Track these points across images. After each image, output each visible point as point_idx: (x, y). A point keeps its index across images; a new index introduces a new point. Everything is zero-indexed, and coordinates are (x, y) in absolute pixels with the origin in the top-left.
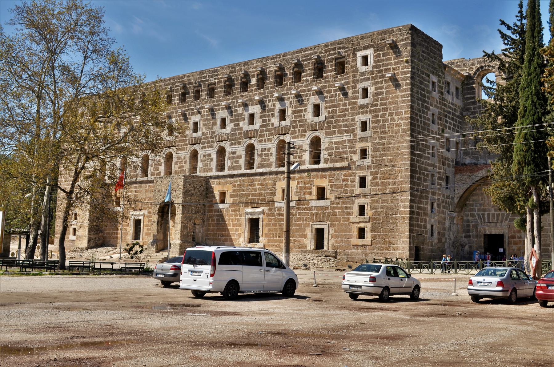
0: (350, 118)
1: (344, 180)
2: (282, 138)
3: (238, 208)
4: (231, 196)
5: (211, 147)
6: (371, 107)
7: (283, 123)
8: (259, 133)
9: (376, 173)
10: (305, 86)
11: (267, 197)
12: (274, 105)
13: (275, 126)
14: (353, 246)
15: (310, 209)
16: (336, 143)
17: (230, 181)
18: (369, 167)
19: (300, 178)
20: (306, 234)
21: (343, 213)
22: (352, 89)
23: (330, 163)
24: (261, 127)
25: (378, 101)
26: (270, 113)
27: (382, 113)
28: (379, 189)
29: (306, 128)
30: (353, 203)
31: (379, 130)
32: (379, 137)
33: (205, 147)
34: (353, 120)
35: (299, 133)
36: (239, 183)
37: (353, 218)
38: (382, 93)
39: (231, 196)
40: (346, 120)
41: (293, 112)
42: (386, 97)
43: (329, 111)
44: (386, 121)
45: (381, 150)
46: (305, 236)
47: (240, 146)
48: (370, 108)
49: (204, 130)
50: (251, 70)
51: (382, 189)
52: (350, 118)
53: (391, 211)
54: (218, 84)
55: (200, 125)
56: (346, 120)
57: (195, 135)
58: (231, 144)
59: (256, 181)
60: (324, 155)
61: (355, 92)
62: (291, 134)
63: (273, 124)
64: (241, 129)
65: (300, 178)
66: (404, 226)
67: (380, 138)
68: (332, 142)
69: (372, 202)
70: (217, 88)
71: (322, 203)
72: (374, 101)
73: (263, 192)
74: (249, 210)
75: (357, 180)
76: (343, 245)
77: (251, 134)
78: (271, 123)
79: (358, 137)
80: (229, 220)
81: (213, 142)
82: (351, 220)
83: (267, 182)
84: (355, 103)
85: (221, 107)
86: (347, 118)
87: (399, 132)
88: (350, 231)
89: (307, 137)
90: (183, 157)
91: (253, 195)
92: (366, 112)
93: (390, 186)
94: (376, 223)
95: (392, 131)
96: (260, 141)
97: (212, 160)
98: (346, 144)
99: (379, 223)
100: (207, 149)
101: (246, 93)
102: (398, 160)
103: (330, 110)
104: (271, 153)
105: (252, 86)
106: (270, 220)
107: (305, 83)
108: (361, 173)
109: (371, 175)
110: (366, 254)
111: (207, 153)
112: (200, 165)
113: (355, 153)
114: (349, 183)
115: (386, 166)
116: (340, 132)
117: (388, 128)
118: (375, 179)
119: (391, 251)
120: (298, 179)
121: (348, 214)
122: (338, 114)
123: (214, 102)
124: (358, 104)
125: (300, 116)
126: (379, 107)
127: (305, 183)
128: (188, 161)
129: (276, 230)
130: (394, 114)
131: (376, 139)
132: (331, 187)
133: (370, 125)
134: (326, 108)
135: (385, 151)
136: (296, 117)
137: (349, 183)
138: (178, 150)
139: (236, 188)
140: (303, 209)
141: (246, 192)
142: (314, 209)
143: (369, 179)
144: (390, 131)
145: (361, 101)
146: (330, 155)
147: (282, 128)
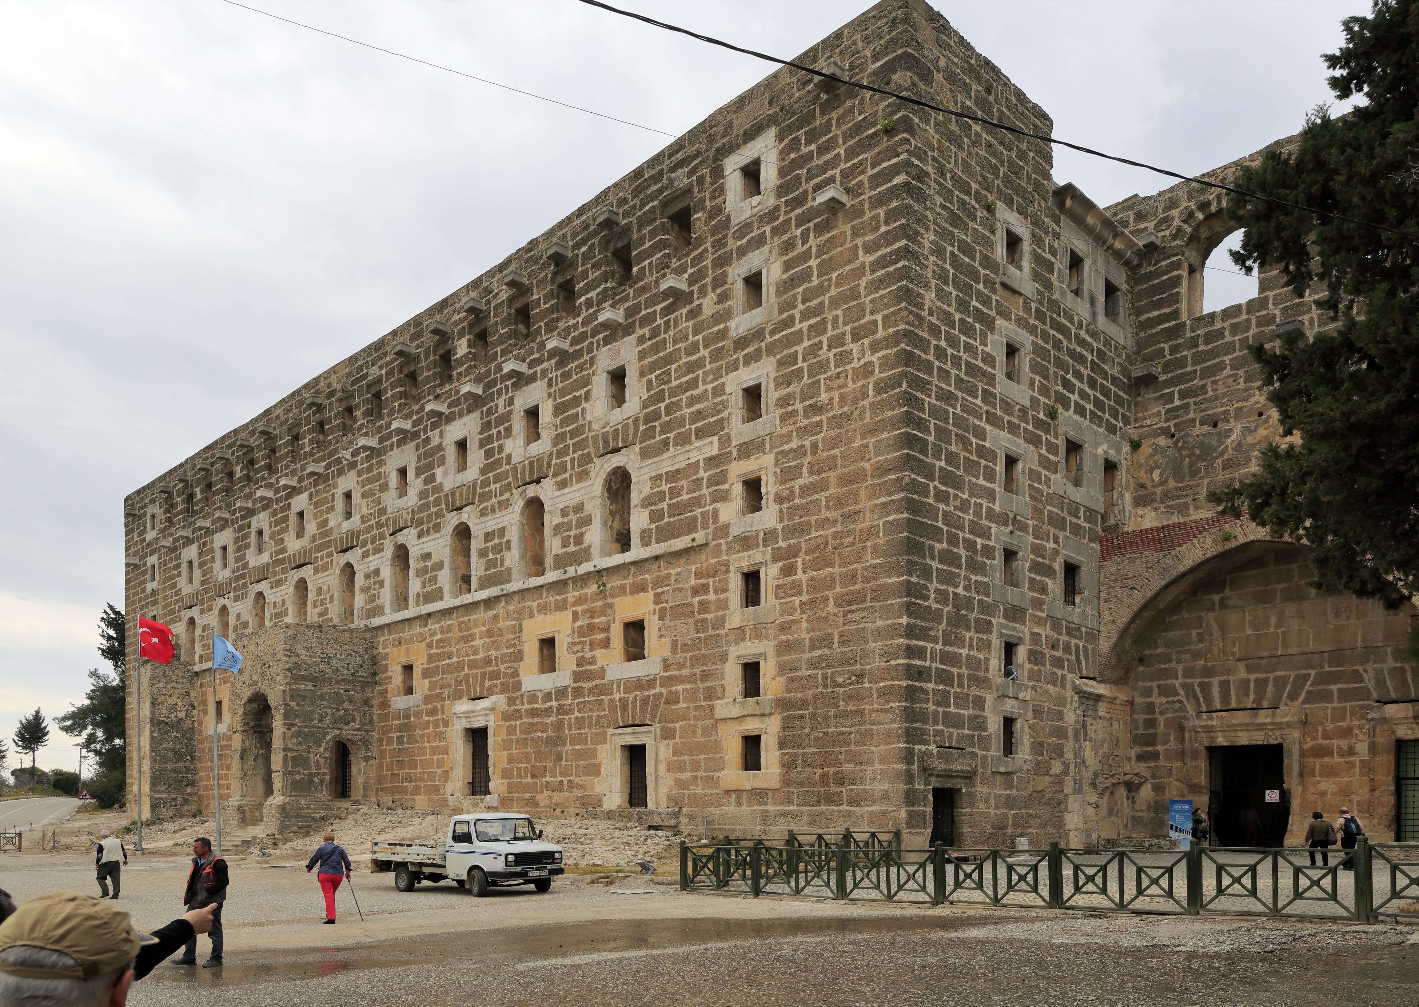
0: (709, 387)
1: (696, 591)
2: (531, 491)
3: (439, 705)
4: (426, 673)
5: (379, 550)
6: (772, 333)
7: (537, 448)
8: (479, 491)
9: (793, 552)
10: (584, 324)
11: (502, 668)
12: (511, 402)
13: (514, 461)
14: (727, 792)
15: (605, 690)
16: (673, 476)
17: (421, 635)
18: (770, 536)
19: (580, 601)
20: (600, 765)
21: (695, 691)
22: (714, 289)
23: (657, 542)
24: (484, 471)
25: (795, 307)
26: (502, 428)
27: (806, 343)
28: (802, 603)
29: (591, 449)
30: (724, 658)
31: (799, 406)
32: (798, 429)
33: (366, 555)
34: (720, 390)
35: (572, 468)
36: (439, 636)
37: (722, 708)
38: (806, 276)
39: (426, 673)
40: (699, 399)
41: (558, 410)
42: (821, 284)
43: (649, 382)
44: (822, 367)
45: (805, 471)
46: (596, 770)
47: (438, 535)
48: (768, 339)
49: (365, 511)
50: (456, 317)
51: (813, 601)
52: (709, 387)
53: (841, 674)
54: (387, 380)
55: (356, 498)
56: (699, 399)
57: (346, 526)
58: (420, 536)
59: (476, 626)
60: (639, 520)
61: (723, 298)
62: (555, 475)
63: (509, 457)
64: (438, 489)
65: (580, 601)
66: (886, 719)
67: (802, 432)
68: (659, 477)
69: (783, 648)
70: (386, 390)
71: (637, 669)
72: (781, 311)
73: (493, 653)
74: (463, 706)
75: (736, 583)
76: (699, 791)
77: (461, 496)
78: (503, 455)
79: (734, 444)
80: (423, 736)
81: (382, 536)
82: (719, 714)
83: (501, 624)
84: (723, 334)
85: (395, 439)
86: (701, 388)
87: (865, 396)
88: (717, 747)
89: (592, 475)
90: (325, 588)
91: (472, 665)
92: (755, 357)
93: (838, 589)
94: (793, 718)
95: (842, 398)
96: (483, 513)
97: (381, 584)
98: (702, 474)
99: (803, 717)
100: (372, 558)
101: (448, 387)
102: (863, 494)
103: (653, 376)
104: (509, 542)
105: (460, 362)
106: (511, 730)
107: (584, 314)
108: (745, 561)
109: (775, 561)
110: (765, 818)
111: (372, 567)
112: (360, 600)
113: (722, 497)
114: (711, 597)
115: (823, 523)
116: (683, 440)
117: (829, 389)
118: (788, 571)
119: (844, 808)
120: (574, 604)
121: (711, 695)
122: (674, 383)
123: (380, 429)
124: (733, 334)
125: (574, 418)
126: (797, 327)
127: (592, 613)
128: (336, 594)
129: (526, 758)
130: (848, 337)
131: (787, 438)
132: (662, 618)
133: (770, 395)
134: (642, 374)
135: (819, 472)
136: (564, 422)
137: (711, 597)
138: (316, 571)
139: (434, 651)
140: (590, 690)
141: (455, 660)
142: (618, 690)
143: (770, 576)
144: (836, 400)
145: (741, 323)
146: (655, 516)
147: (531, 463)
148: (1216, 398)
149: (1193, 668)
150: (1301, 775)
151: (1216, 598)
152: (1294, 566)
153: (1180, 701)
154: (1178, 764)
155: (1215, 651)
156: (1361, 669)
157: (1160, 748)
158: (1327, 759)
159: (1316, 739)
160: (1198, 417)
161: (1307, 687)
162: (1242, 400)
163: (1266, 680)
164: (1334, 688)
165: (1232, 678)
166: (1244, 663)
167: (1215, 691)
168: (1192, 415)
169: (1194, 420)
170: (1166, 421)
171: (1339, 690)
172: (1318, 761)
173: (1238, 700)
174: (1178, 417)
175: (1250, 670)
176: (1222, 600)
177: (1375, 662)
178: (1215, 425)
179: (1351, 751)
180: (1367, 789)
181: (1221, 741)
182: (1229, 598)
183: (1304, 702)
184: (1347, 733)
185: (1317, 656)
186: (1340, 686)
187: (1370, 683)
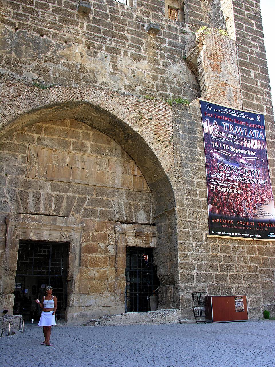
148: (43, 21)
149: (17, 179)
150: (80, 265)
151: (36, 136)
152: (81, 131)
153: (6, 203)
156: (111, 199)
159: (88, 241)
160: (33, 26)
161: (85, 206)
162: (58, 30)
163: (63, 197)
164: (99, 209)
165: (42, 192)
166: (50, 183)
167: (31, 199)
168: (29, 23)
169: (30, 26)
170: (14, 18)
171: (101, 211)
172: (89, 256)
174: (21, 20)
175: (53, 188)
176: (39, 138)
177: (118, 197)
178: (42, 36)
179: (106, 251)
180: (114, 276)
181: (32, 236)
182: (43, 138)
184: (104, 238)
185: (90, 187)
186: (101, 209)
187: (115, 210)
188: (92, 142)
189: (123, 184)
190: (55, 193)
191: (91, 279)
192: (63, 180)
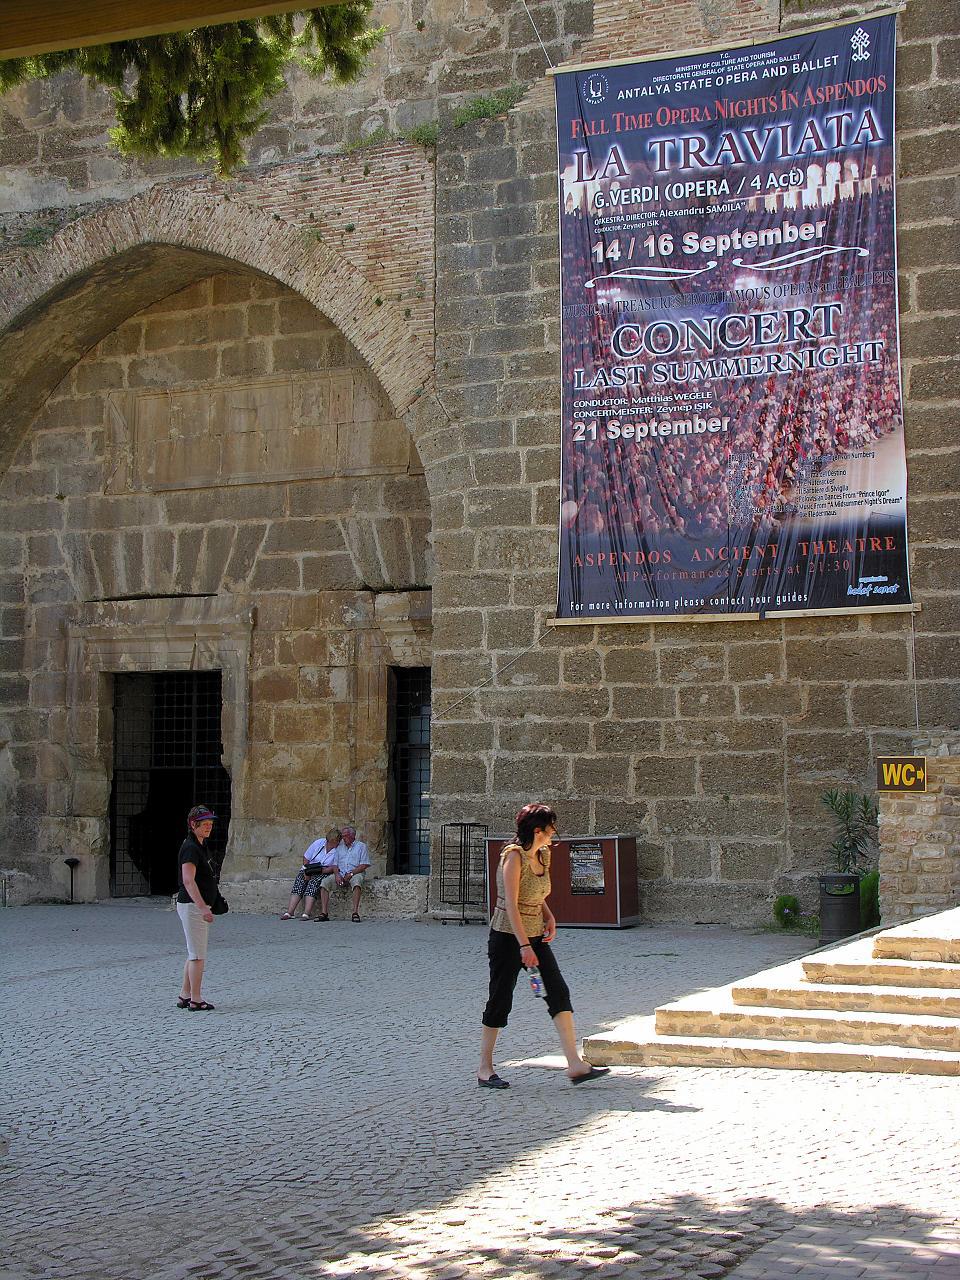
150: (249, 735)
151: (125, 361)
152: (243, 307)
153: (63, 576)
154: (57, 709)
155: (121, 473)
156: (336, 518)
157: (30, 675)
158: (286, 704)
161: (259, 554)
164: (299, 557)
167: (119, 551)
172: (273, 707)
173: (156, 581)
175: (175, 514)
176: (133, 366)
177: (359, 508)
179: (323, 690)
180: (346, 768)
181: (127, 663)
182: (144, 363)
183: (255, 585)
187: (352, 552)
188: (278, 336)
189: (377, 459)
190: (177, 528)
191: (280, 776)
192: (196, 482)
